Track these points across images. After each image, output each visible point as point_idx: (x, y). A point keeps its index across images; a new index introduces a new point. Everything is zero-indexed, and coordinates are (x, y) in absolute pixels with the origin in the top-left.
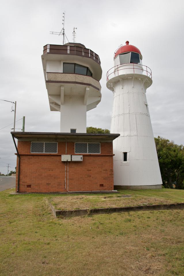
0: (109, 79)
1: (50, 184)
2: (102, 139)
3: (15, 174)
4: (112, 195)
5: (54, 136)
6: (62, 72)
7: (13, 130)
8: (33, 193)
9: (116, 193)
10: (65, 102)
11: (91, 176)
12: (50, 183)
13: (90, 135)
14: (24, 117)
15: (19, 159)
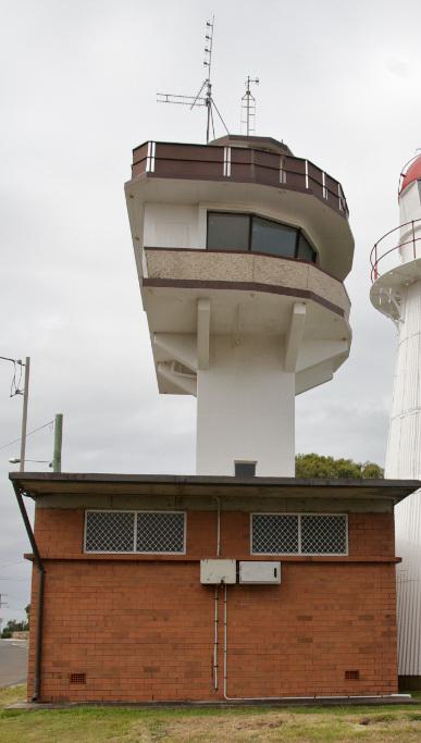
0: (382, 271)
1: (157, 670)
2: (354, 500)
3: (25, 633)
4: (392, 713)
5: (172, 490)
6: (204, 247)
7: (19, 464)
8: (91, 703)
9: (407, 703)
10: (214, 360)
11: (310, 640)
12: (156, 664)
13: (309, 486)
14: (60, 418)
15: (39, 575)
